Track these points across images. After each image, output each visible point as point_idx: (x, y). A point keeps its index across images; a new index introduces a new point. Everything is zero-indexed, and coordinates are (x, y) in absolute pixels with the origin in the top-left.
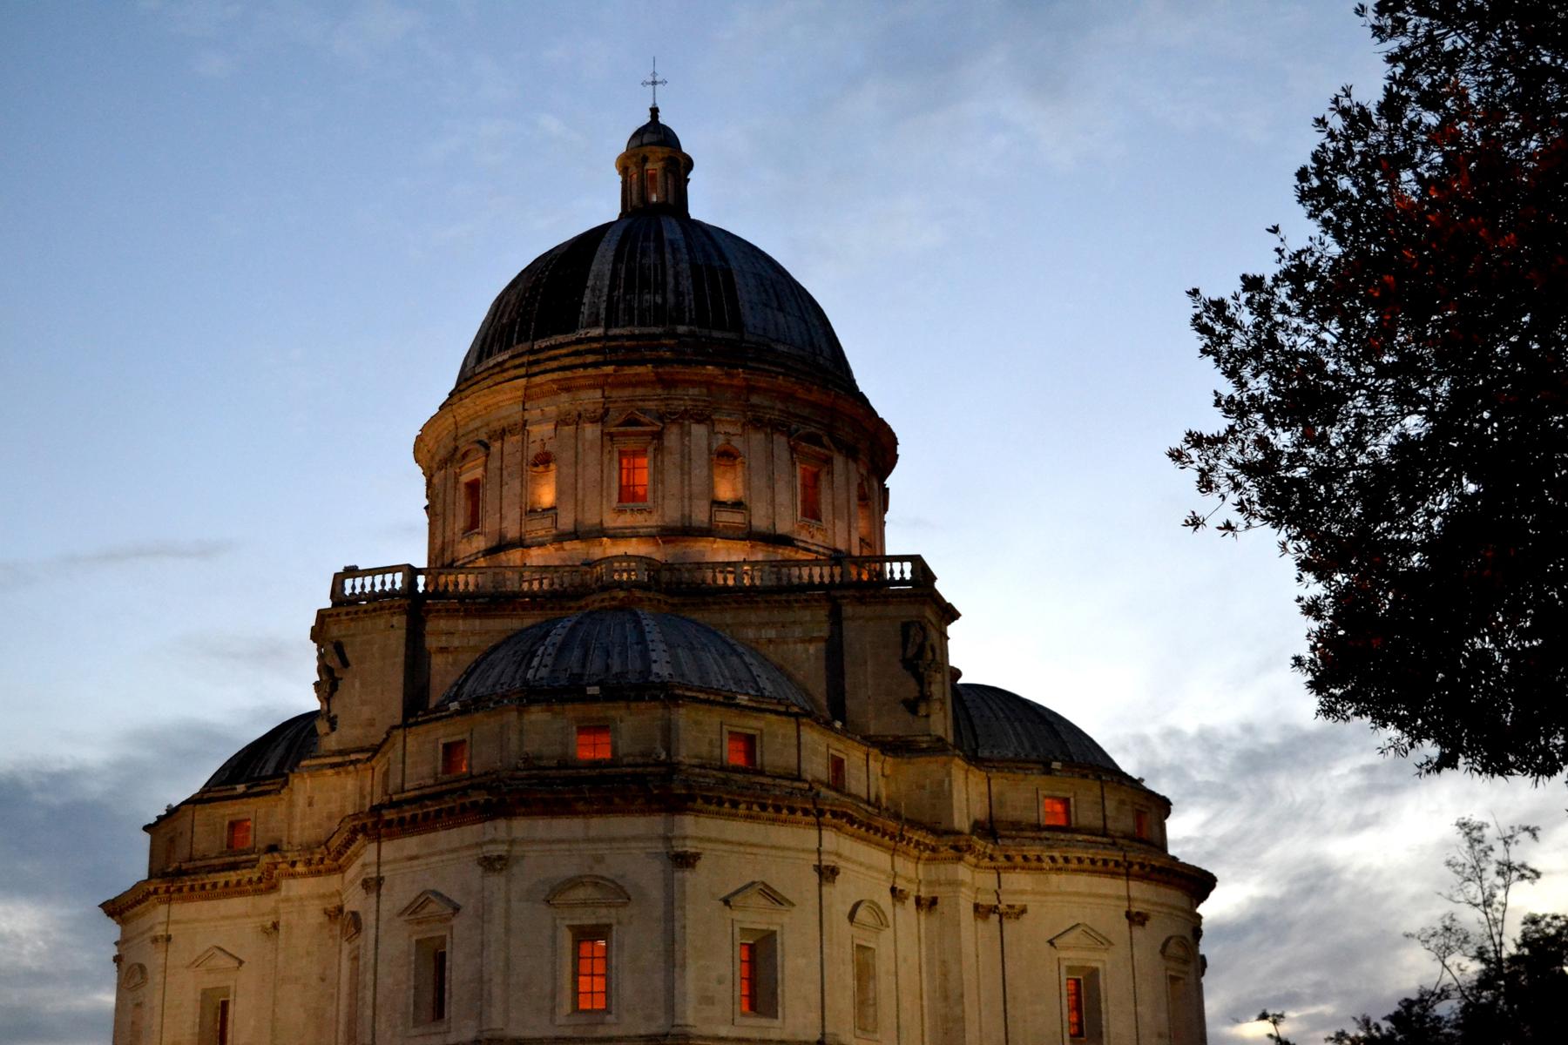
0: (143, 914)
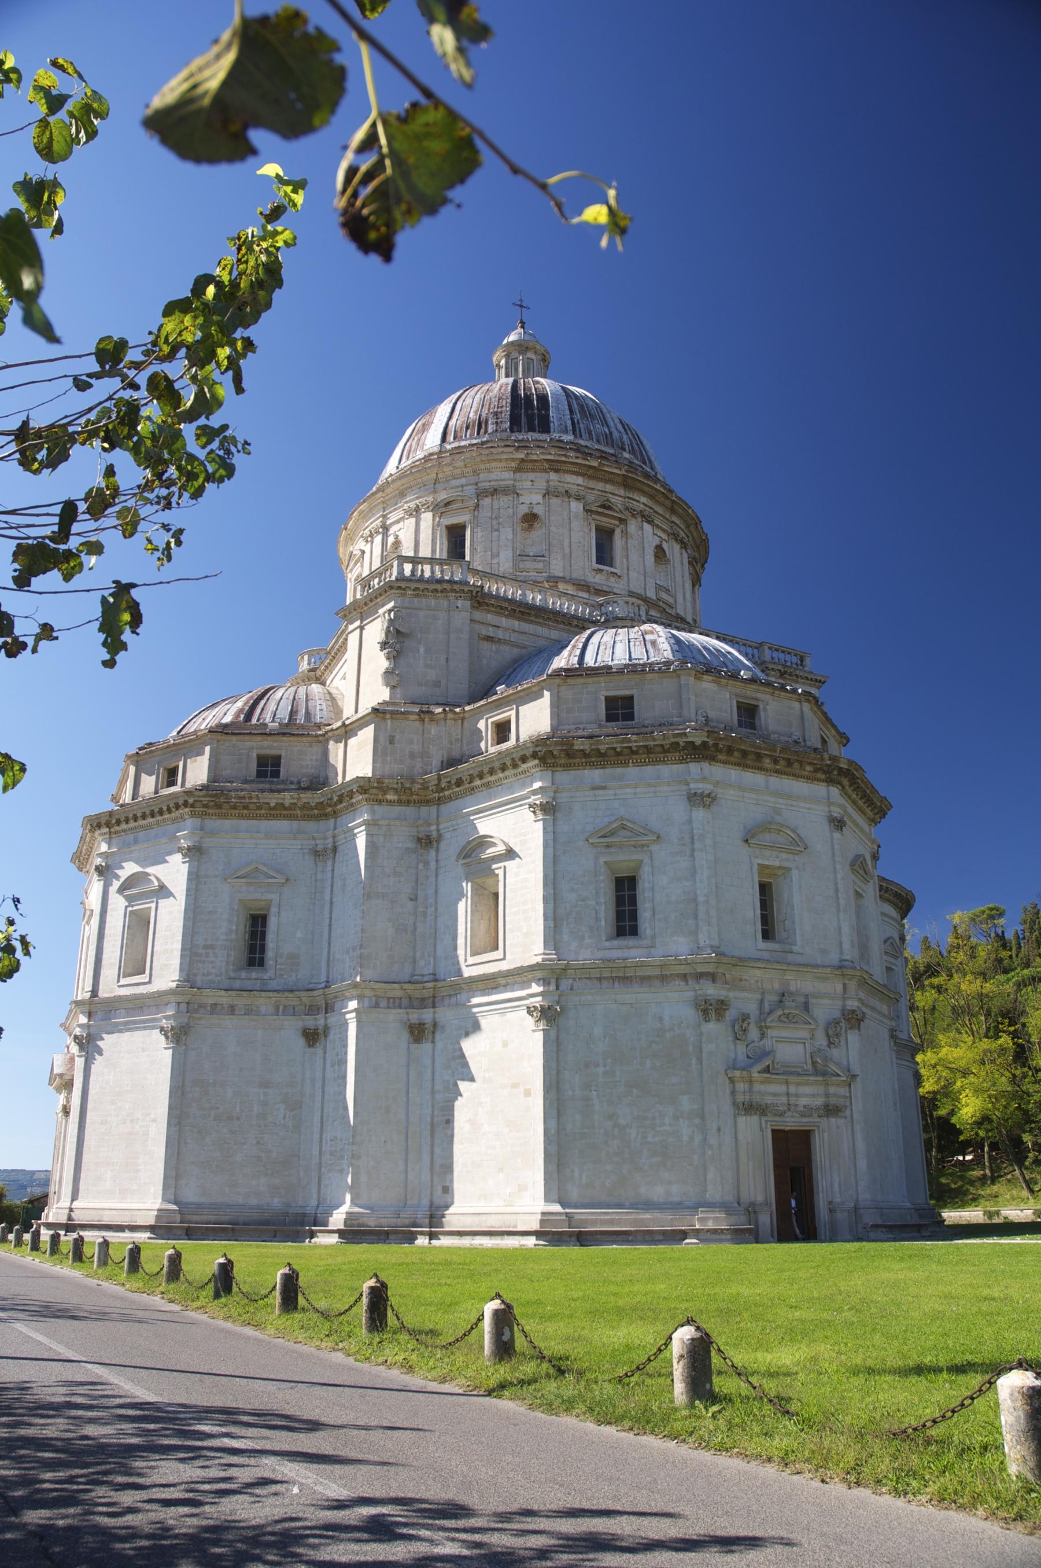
0: (150, 827)
